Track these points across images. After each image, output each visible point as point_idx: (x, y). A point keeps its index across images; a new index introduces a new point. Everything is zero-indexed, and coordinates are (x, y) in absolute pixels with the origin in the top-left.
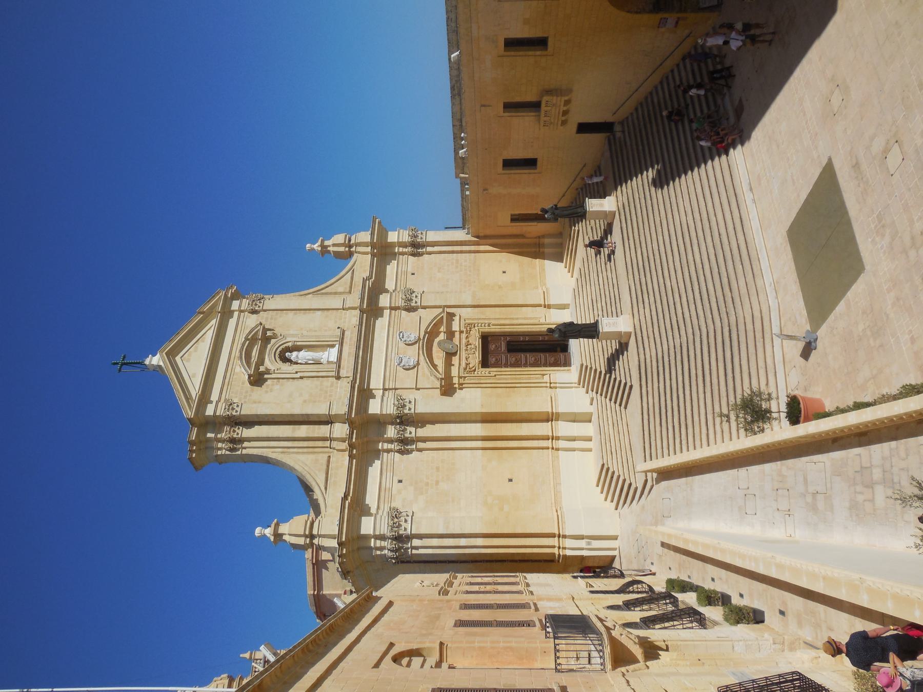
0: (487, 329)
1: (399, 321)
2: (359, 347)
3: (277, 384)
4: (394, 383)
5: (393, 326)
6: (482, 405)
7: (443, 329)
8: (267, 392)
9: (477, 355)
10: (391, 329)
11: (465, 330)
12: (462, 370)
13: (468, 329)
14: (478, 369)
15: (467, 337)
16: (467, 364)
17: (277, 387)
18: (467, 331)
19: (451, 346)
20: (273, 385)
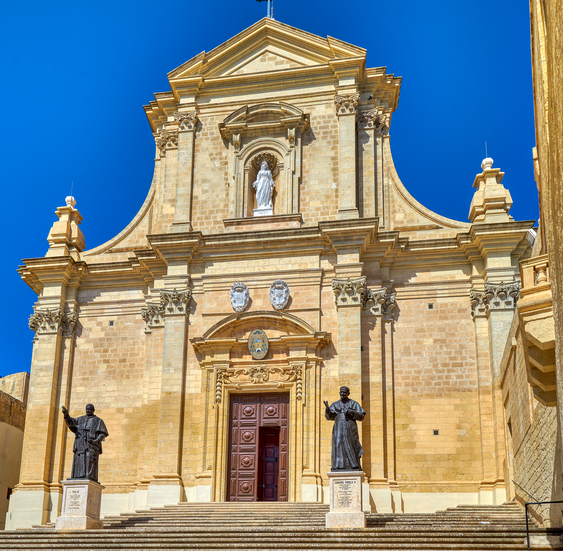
0: (293, 396)
1: (312, 283)
2: (259, 236)
3: (221, 163)
4: (211, 289)
5: (302, 276)
6: (170, 393)
7: (293, 336)
8: (211, 155)
9: (248, 385)
10: (298, 275)
11: (290, 366)
12: (222, 366)
13: (291, 371)
14: (225, 387)
15: (277, 370)
16: (233, 373)
17: (217, 164)
18: (289, 370)
19: (260, 349)
20: (221, 159)
